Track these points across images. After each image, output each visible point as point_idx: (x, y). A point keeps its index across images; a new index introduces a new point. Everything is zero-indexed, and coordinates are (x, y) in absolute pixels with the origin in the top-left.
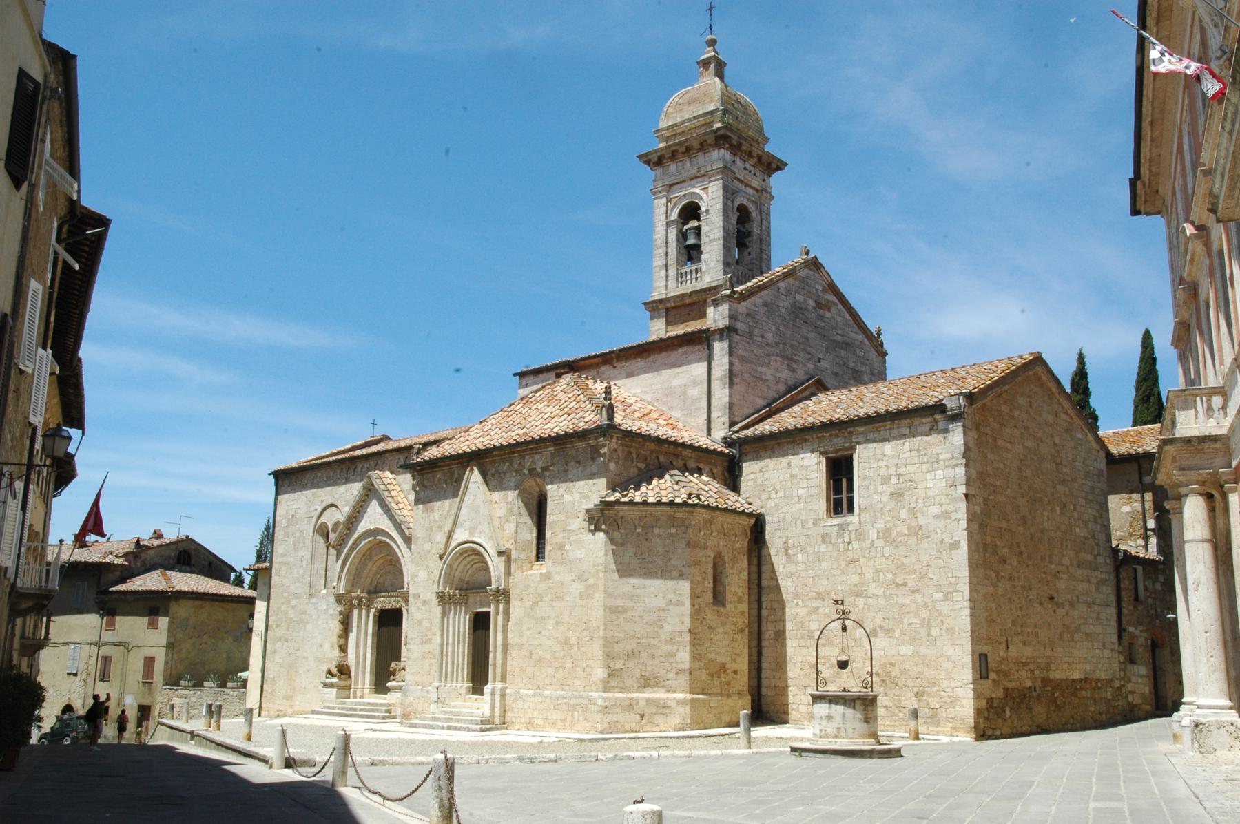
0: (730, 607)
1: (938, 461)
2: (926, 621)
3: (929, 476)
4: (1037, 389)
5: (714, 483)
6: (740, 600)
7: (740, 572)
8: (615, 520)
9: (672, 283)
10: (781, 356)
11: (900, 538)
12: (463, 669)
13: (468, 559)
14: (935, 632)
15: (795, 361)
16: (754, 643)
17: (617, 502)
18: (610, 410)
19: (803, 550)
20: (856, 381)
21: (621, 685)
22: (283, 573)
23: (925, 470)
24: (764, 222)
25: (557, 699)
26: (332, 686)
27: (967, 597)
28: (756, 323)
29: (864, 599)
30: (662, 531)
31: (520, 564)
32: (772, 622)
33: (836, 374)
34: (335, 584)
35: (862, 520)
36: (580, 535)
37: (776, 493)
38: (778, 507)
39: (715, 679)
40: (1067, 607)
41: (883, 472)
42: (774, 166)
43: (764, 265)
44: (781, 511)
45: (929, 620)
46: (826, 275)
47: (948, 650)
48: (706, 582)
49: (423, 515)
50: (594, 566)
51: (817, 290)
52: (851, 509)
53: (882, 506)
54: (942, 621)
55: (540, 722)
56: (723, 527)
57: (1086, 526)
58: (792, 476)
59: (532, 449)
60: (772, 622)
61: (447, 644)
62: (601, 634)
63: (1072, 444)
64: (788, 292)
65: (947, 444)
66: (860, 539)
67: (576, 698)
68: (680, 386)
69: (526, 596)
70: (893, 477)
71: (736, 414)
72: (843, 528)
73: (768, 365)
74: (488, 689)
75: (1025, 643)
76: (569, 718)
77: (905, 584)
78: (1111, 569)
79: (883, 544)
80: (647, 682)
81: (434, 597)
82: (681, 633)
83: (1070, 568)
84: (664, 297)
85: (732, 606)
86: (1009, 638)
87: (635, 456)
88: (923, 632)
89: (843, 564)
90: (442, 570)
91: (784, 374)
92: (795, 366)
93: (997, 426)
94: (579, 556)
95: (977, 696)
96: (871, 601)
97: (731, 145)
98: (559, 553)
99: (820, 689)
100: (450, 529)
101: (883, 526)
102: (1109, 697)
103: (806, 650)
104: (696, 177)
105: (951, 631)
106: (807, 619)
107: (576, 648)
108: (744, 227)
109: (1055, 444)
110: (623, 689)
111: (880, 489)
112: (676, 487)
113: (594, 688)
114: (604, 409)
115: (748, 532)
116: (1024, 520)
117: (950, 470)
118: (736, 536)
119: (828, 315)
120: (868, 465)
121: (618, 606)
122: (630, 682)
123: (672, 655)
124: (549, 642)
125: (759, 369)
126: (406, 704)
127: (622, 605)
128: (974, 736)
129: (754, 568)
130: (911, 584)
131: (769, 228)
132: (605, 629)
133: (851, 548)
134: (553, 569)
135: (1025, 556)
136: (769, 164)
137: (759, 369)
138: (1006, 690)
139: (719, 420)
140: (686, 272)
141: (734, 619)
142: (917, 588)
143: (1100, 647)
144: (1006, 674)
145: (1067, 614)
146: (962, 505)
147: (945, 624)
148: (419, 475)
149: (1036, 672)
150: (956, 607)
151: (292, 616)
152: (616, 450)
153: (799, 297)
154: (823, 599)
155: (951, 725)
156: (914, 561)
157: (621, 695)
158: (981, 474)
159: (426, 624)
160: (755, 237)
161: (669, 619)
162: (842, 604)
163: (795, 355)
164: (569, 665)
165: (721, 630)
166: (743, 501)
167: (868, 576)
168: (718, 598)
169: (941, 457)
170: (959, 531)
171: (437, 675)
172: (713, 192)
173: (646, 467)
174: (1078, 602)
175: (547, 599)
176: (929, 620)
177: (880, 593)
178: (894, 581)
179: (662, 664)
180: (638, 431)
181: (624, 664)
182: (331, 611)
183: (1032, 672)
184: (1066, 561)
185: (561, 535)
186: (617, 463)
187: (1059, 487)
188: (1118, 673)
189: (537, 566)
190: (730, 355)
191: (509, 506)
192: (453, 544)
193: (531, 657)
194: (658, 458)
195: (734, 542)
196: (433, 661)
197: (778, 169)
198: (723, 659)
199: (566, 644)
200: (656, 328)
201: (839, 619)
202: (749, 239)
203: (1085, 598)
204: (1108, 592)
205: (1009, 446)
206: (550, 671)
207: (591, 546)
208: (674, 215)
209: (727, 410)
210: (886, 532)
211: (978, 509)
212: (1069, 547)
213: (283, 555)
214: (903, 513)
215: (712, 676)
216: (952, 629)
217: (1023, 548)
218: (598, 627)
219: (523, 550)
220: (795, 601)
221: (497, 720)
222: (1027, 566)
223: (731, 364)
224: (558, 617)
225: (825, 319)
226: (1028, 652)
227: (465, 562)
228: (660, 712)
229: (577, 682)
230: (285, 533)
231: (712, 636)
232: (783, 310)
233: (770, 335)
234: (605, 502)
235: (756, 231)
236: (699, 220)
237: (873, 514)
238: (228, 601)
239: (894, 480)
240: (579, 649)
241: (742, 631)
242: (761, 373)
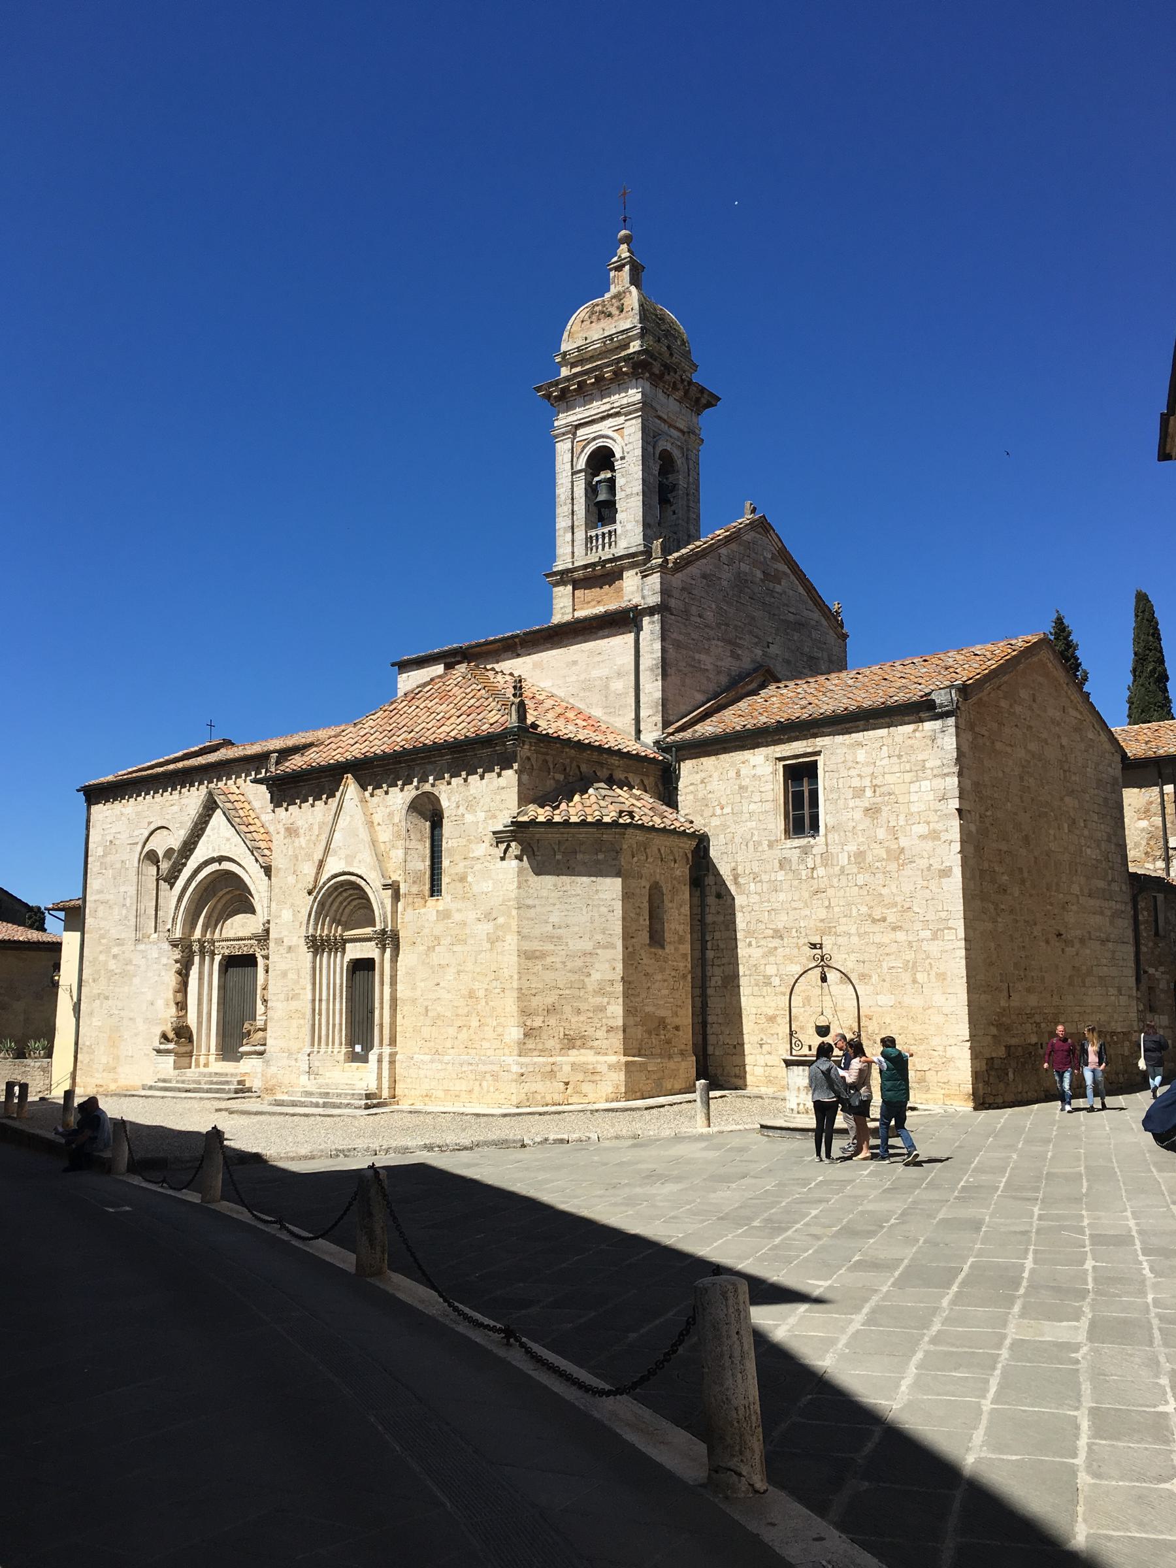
0: (669, 949)
1: (924, 768)
2: (910, 964)
3: (914, 787)
4: (1041, 679)
5: (646, 797)
6: (681, 940)
7: (681, 906)
8: (529, 844)
9: (580, 549)
10: (723, 640)
11: (877, 864)
12: (341, 1030)
13: (345, 894)
14: (920, 977)
15: (740, 646)
16: (698, 991)
17: (533, 823)
18: (522, 709)
19: (756, 877)
20: (811, 670)
21: (540, 1047)
22: (100, 914)
23: (907, 780)
24: (692, 473)
25: (461, 1065)
26: (168, 1052)
27: (962, 934)
28: (693, 599)
29: (833, 938)
30: (587, 857)
31: (410, 900)
32: (718, 966)
33: (788, 662)
34: (169, 926)
35: (829, 841)
36: (486, 864)
37: (722, 808)
38: (724, 826)
39: (653, 1036)
40: (1077, 945)
41: (856, 782)
42: (704, 401)
43: (691, 527)
44: (728, 830)
45: (915, 963)
46: (776, 540)
47: (939, 999)
48: (641, 918)
49: (285, 841)
50: (504, 901)
51: (765, 558)
52: (815, 827)
53: (854, 824)
54: (930, 964)
55: (441, 1094)
56: (659, 850)
57: (1099, 846)
58: (741, 787)
59: (422, 758)
60: (718, 966)
61: (320, 1000)
62: (515, 985)
63: (1082, 746)
64: (731, 561)
65: (935, 748)
66: (827, 864)
67: (484, 1064)
68: (601, 678)
69: (419, 939)
70: (867, 789)
71: (670, 712)
72: (806, 850)
73: (707, 651)
74: (373, 1056)
75: (1029, 990)
76: (477, 1089)
77: (884, 920)
78: (1127, 898)
79: (855, 870)
80: (571, 1042)
81: (302, 941)
82: (612, 982)
83: (1080, 897)
84: (570, 566)
85: (673, 948)
86: (1011, 985)
87: (551, 766)
88: (906, 978)
89: (806, 895)
91: (727, 663)
92: (740, 652)
93: (995, 726)
94: (486, 890)
95: (975, 1055)
96: (840, 940)
97: (652, 374)
98: (459, 885)
99: (794, 1053)
100: (320, 857)
101: (855, 848)
102: (1127, 1053)
103: (761, 999)
104: (609, 416)
105: (942, 977)
106: (763, 962)
107: (483, 1002)
108: (667, 479)
109: (1062, 747)
110: (543, 1052)
111: (851, 803)
112: (603, 803)
113: (507, 1051)
114: (514, 706)
115: (690, 856)
116: (1026, 839)
117: (939, 780)
118: (675, 862)
119: (778, 588)
120: (836, 775)
121: (535, 951)
122: (551, 1043)
123: (602, 1009)
124: (449, 996)
125: (697, 656)
126: (269, 1075)
127: (541, 948)
128: (971, 1104)
129: (696, 901)
130: (891, 918)
131: (698, 480)
132: (520, 979)
133: (815, 876)
134: (453, 906)
135: (1028, 884)
136: (698, 400)
137: (697, 656)
138: (1008, 1047)
139: (650, 719)
140: (597, 536)
141: (675, 963)
142: (900, 924)
143: (1116, 993)
144: (1008, 1029)
145: (1077, 954)
146: (956, 823)
147: (935, 969)
148: (279, 791)
149: (1043, 1025)
150: (947, 948)
151: (114, 967)
152: (528, 758)
153: (744, 567)
154: (781, 937)
155: (943, 1092)
156: (895, 890)
157: (541, 1059)
158: (976, 784)
159: (292, 976)
160: (681, 492)
161: (597, 966)
162: (821, 948)
163: (740, 638)
164: (475, 1023)
165: (659, 977)
166: (682, 820)
167: (837, 909)
168: (656, 938)
169: (928, 765)
170: (951, 856)
171: (308, 1039)
172: (630, 435)
173: (565, 778)
174: (1090, 939)
175: (445, 942)
176: (915, 963)
177: (853, 931)
178: (870, 916)
179: (590, 1020)
180: (555, 735)
181: (544, 1022)
182: (164, 960)
183: (1038, 1024)
184: (1075, 889)
185: (462, 865)
186: (530, 774)
187: (1067, 799)
188: (1135, 1024)
189: (431, 902)
190: (663, 639)
191: (396, 828)
192: (325, 877)
194: (579, 767)
195: (673, 869)
196: (302, 1022)
197: (709, 405)
198: (662, 1013)
199: (471, 997)
200: (562, 605)
201: (817, 966)
202: (674, 494)
203: (1098, 934)
204: (1124, 926)
205: (1009, 749)
206: (452, 1031)
207: (501, 876)
208: (581, 464)
209: (660, 708)
210: (860, 855)
211: (973, 828)
212: (1079, 872)
213: (100, 892)
214: (881, 834)
215: (650, 1033)
216: (944, 974)
217: (1026, 875)
218: (511, 977)
219: (414, 882)
220: (748, 940)
221: (385, 1094)
222: (1031, 895)
223: (663, 650)
224: (459, 965)
225: (776, 595)
226: (1033, 1000)
227: (340, 898)
228: (588, 1079)
229: (486, 1044)
230: (101, 863)
231: (649, 984)
232: (725, 583)
233: (709, 615)
234: (517, 822)
235: (682, 483)
236: (613, 470)
237: (842, 834)
238: (29, 949)
239: (869, 793)
240: (487, 1003)
241: (684, 976)
242: (699, 661)
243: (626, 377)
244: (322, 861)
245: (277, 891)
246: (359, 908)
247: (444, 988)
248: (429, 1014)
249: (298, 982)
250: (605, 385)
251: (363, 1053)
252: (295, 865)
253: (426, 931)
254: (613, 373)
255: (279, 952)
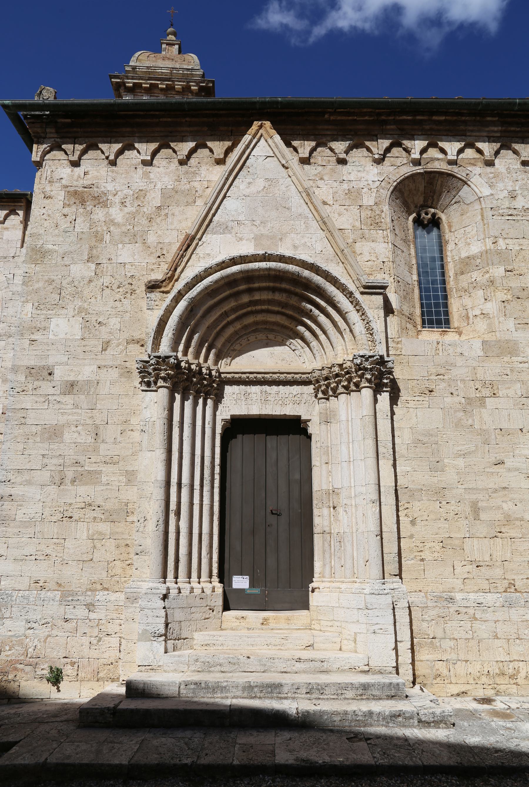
49: (66, 211)
90: (169, 312)
175: (511, 393)
193: (477, 517)
243: (190, 94)
244: (193, 238)
245: (41, 284)
246: (254, 331)
247: (517, 469)
248: (483, 516)
249: (96, 450)
250: (171, 94)
251: (256, 591)
252: (91, 248)
253: (459, 372)
254: (183, 88)
255: (39, 392)
